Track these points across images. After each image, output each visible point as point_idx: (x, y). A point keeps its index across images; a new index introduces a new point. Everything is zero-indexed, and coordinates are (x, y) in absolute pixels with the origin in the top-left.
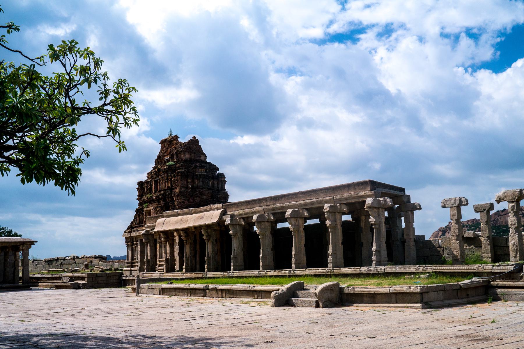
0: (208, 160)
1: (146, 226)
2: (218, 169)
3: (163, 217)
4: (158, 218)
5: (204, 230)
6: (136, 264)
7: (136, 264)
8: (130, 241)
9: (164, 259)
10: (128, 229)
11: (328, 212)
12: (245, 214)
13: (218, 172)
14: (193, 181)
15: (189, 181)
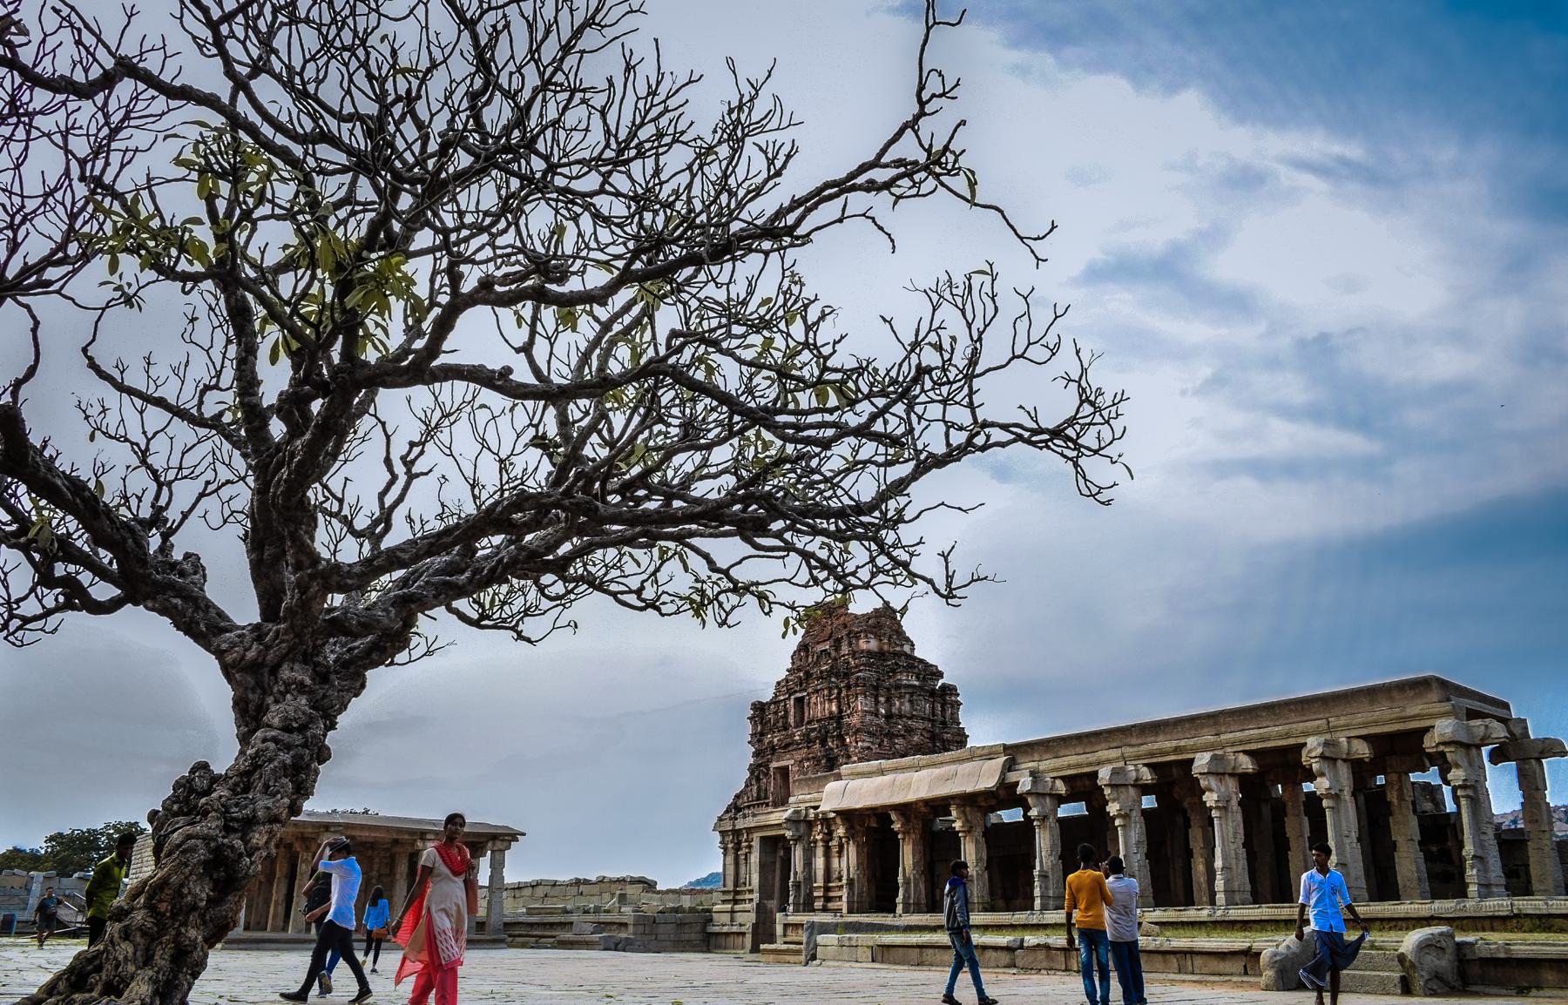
0: (917, 654)
1: (792, 800)
2: (941, 675)
3: (839, 777)
4: (826, 780)
5: (959, 806)
6: (748, 896)
7: (748, 896)
8: (734, 841)
9: (844, 881)
10: (727, 811)
11: (1322, 757)
12: (1069, 767)
13: (940, 683)
14: (888, 700)
15: (882, 699)
